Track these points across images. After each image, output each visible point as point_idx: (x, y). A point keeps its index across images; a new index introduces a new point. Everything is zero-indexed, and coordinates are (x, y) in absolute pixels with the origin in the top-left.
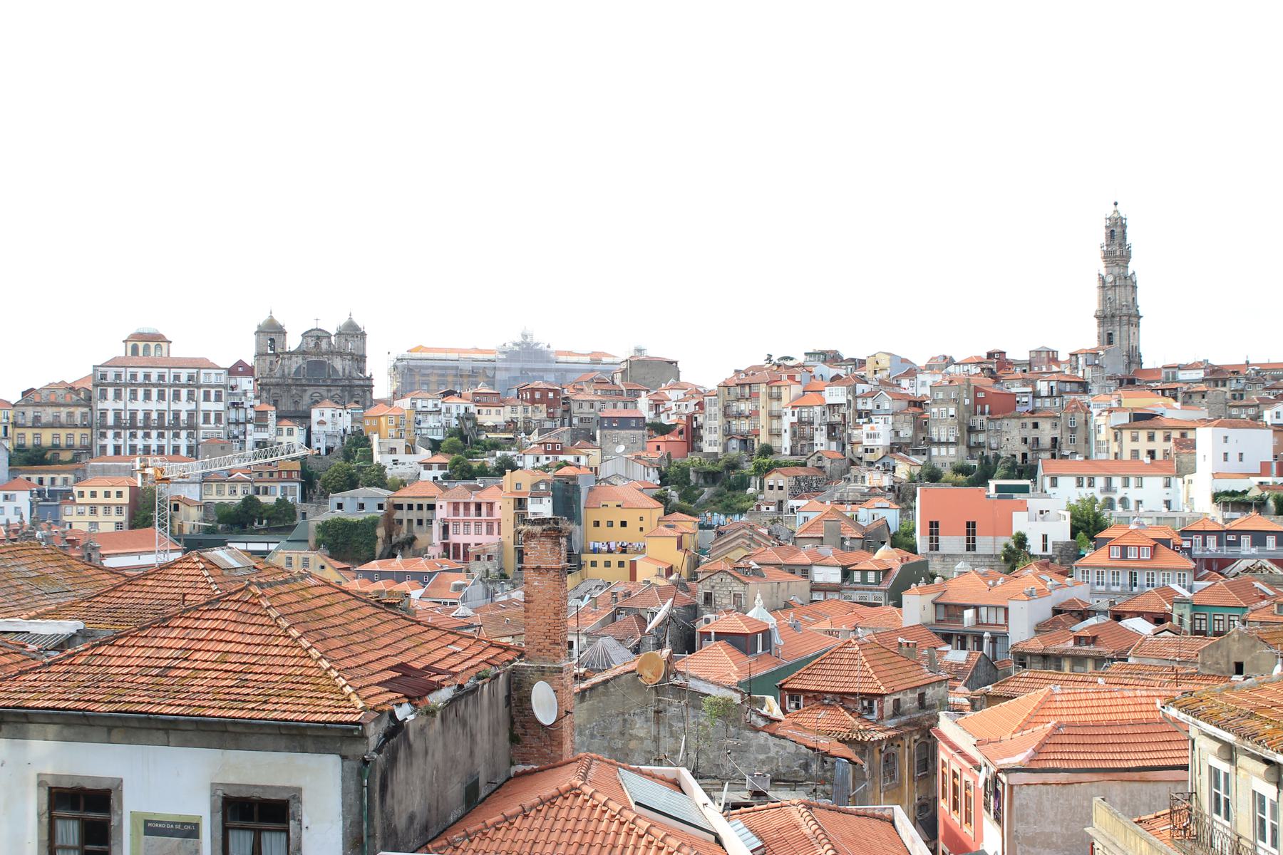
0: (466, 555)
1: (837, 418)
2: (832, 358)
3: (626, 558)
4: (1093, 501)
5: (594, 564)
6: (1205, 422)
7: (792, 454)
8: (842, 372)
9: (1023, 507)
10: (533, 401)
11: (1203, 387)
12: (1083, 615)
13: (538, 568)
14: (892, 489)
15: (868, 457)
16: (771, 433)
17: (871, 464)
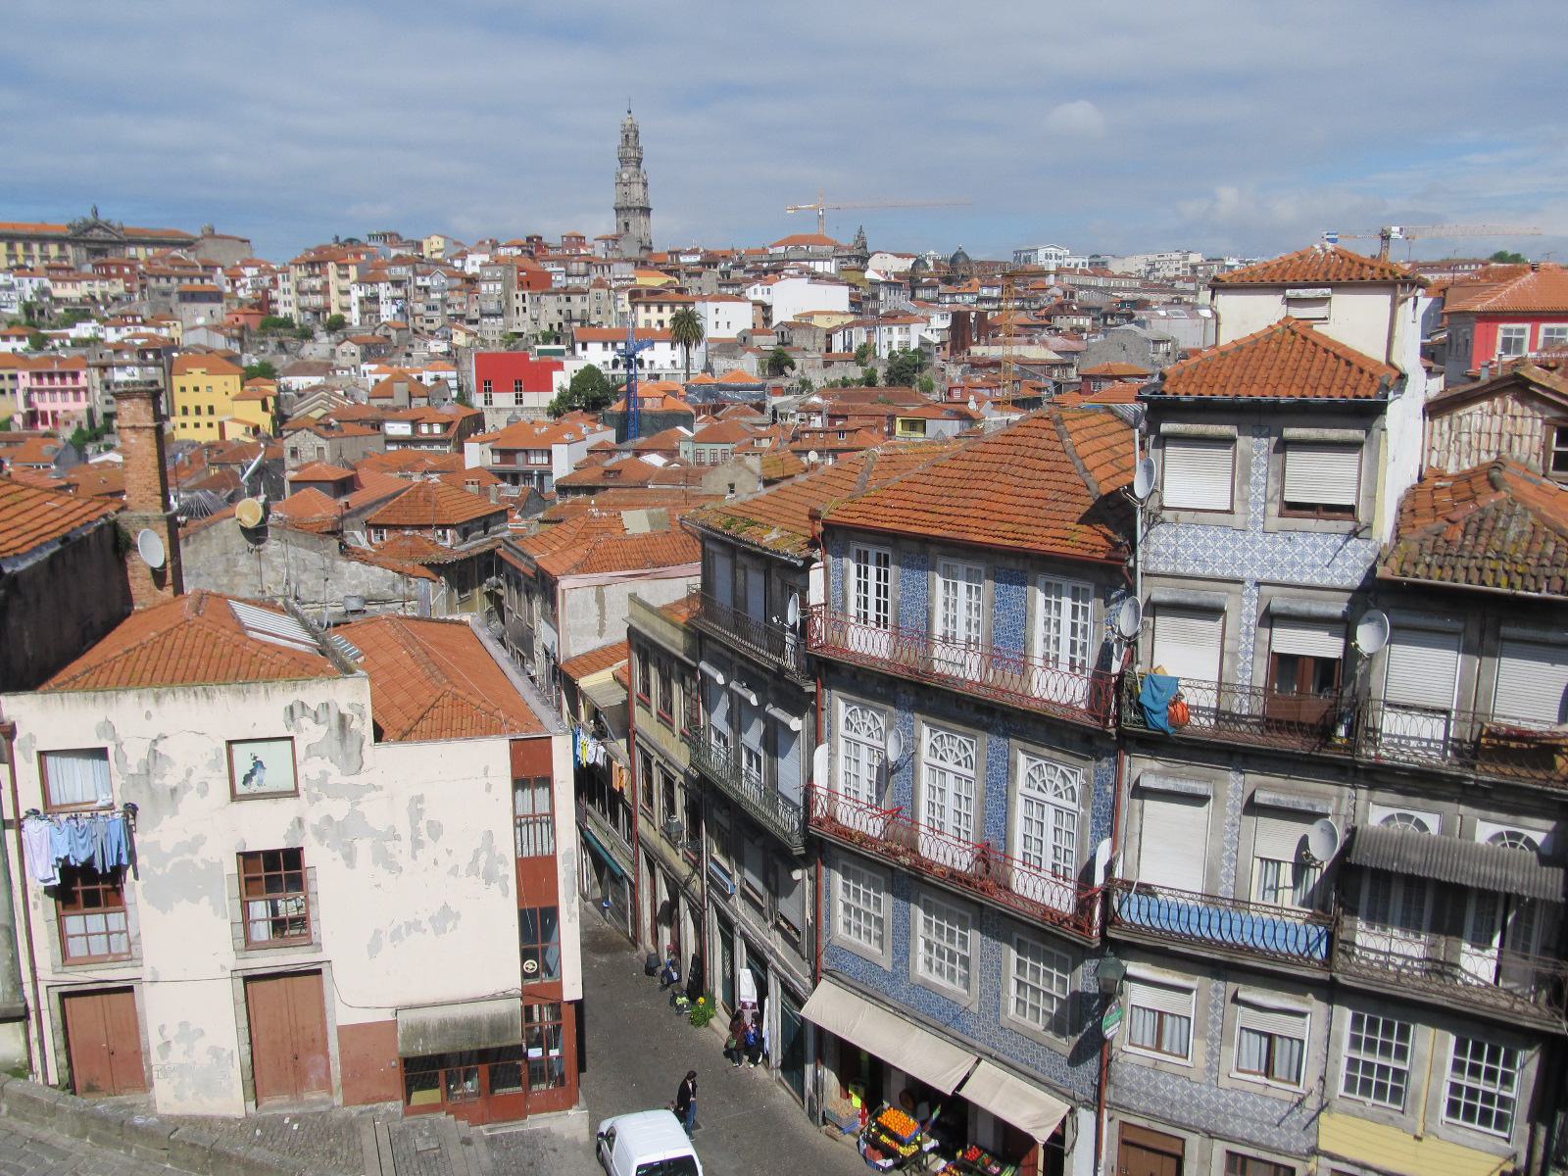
0: (55, 421)
2: (391, 238)
3: (215, 420)
4: (615, 364)
5: (184, 426)
6: (704, 299)
8: (402, 252)
9: (560, 366)
10: (108, 277)
11: (698, 268)
12: (611, 453)
13: (134, 427)
14: (448, 354)
15: (429, 326)
16: (342, 308)
17: (432, 333)
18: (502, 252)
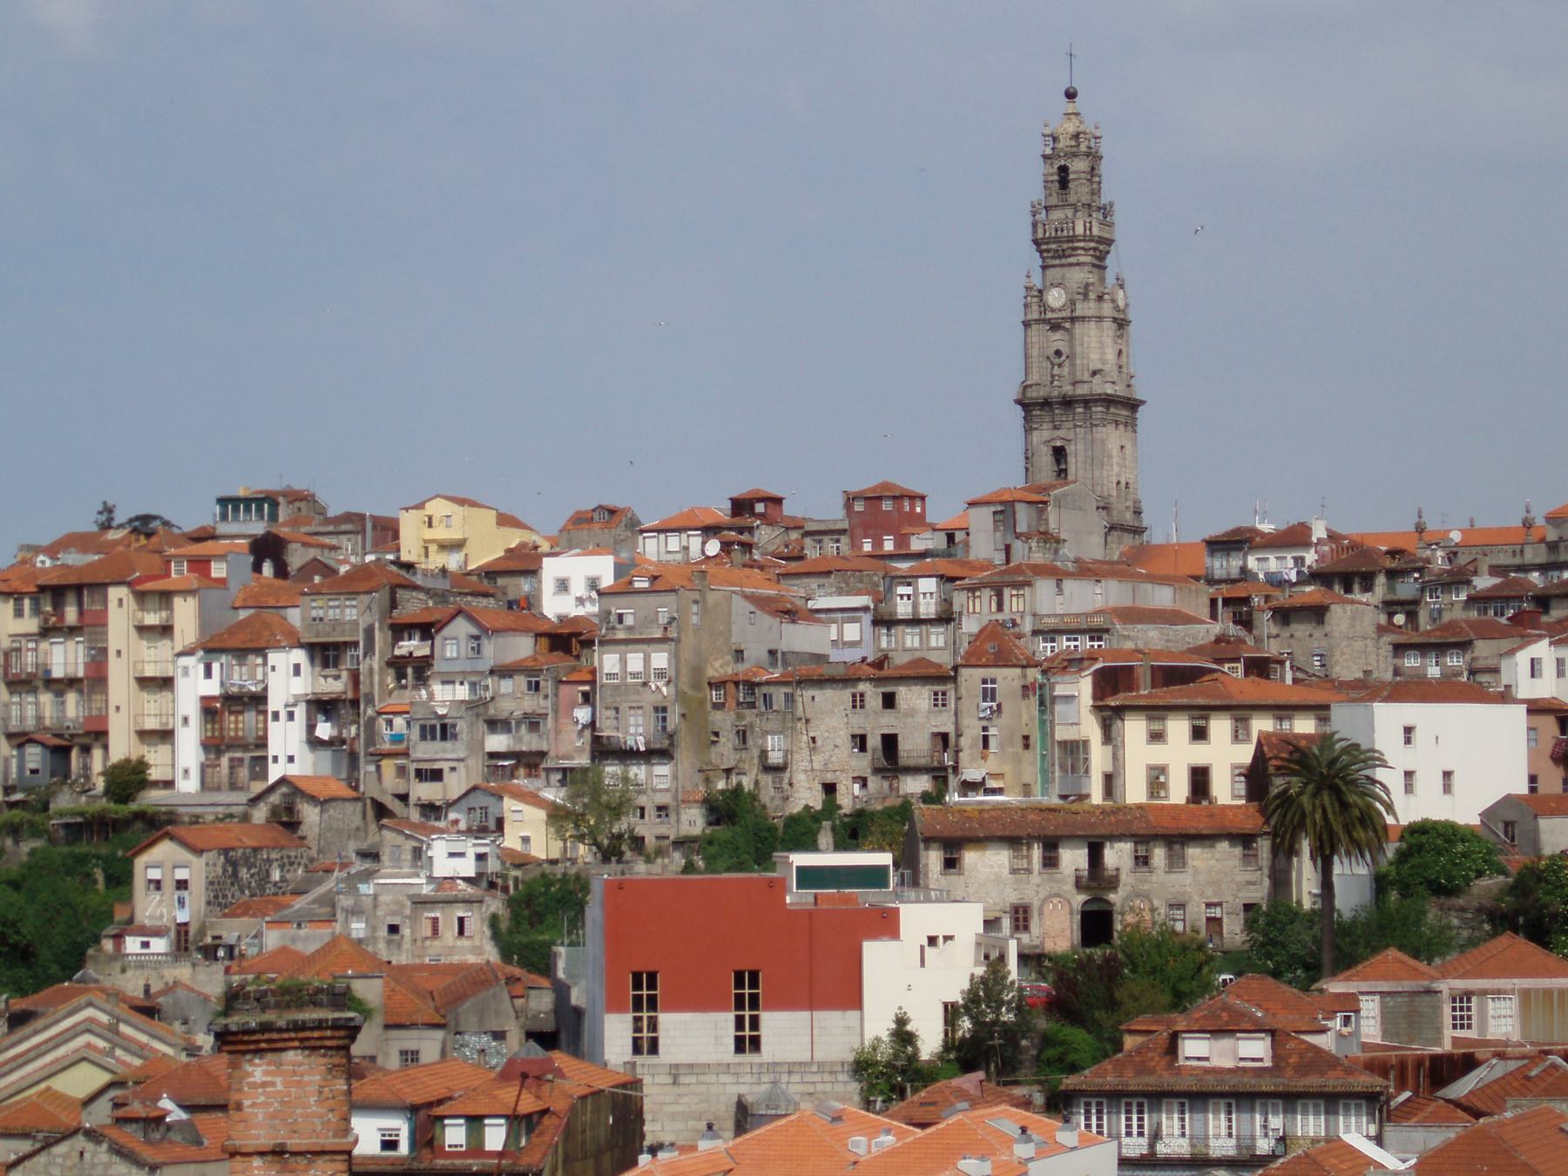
1: (334, 686)
7: (204, 785)
9: (887, 924)
15: (425, 791)
17: (431, 810)
18: (651, 548)
